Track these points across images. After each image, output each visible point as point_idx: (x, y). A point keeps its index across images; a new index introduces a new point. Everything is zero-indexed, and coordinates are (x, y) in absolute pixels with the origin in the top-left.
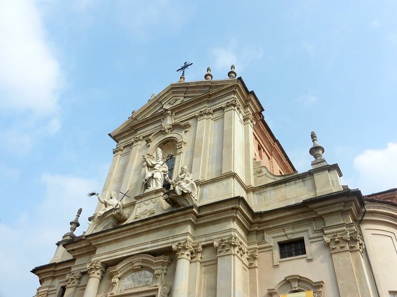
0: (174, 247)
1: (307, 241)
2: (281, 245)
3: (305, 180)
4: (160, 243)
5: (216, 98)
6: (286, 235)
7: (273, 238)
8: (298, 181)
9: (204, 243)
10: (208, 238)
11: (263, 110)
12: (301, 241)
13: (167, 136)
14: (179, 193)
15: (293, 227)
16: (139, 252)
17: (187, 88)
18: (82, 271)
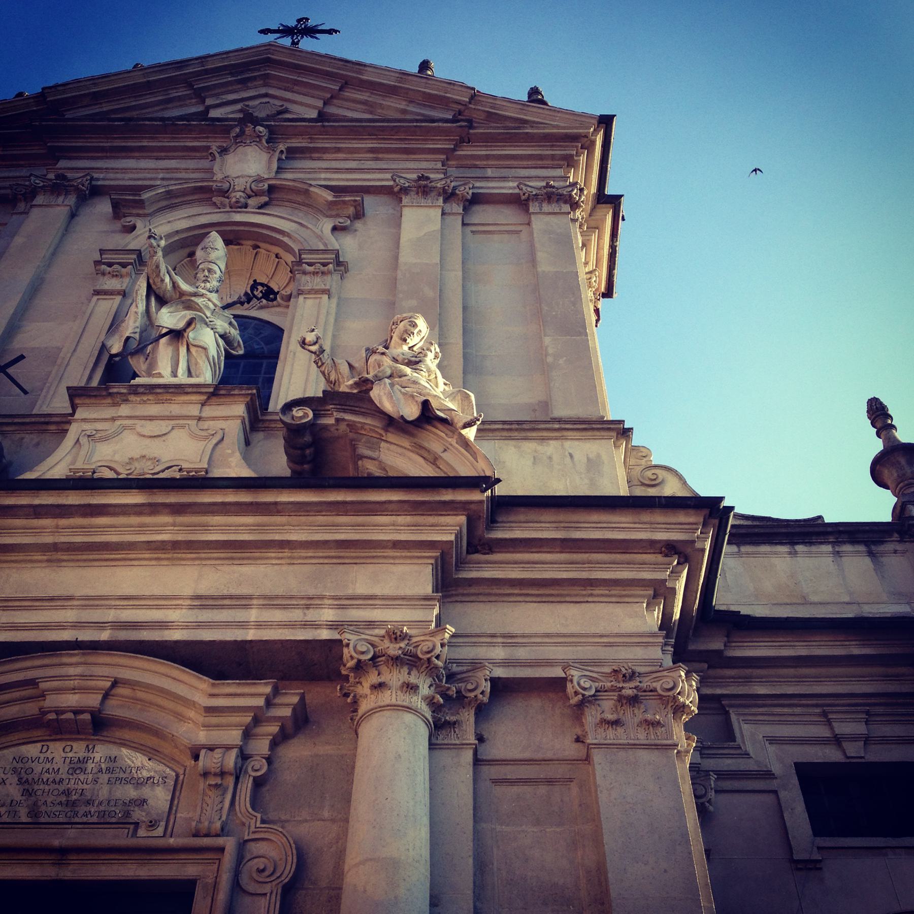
3: (883, 554)
5: (488, 157)
7: (773, 740)
8: (847, 548)
9: (499, 672)
10: (522, 653)
15: (867, 713)
16: (105, 636)
17: (346, 83)
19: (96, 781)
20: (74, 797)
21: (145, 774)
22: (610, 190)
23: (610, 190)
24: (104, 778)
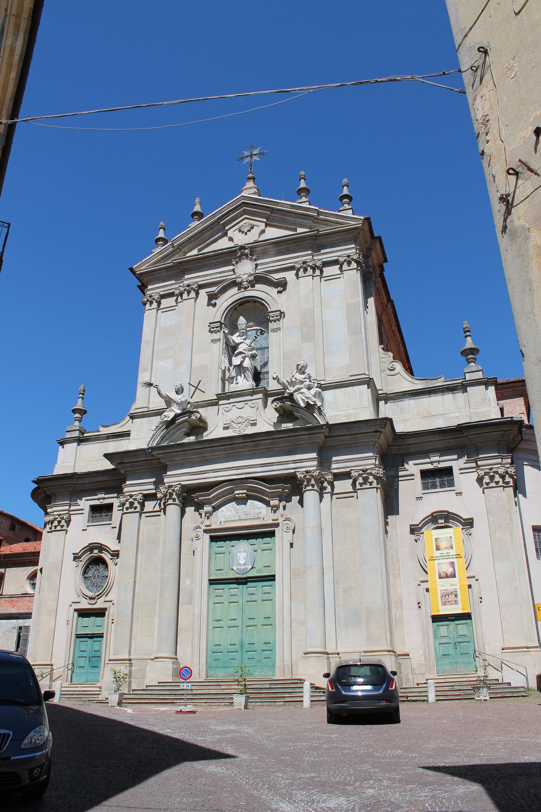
0: (299, 476)
1: (456, 471)
2: (425, 474)
4: (275, 468)
6: (432, 463)
11: (386, 261)
12: (449, 471)
13: (247, 294)
14: (303, 405)
18: (144, 492)
19: (250, 508)
20: (246, 513)
21: (260, 506)
22: (376, 235)
23: (376, 235)
24: (252, 508)
